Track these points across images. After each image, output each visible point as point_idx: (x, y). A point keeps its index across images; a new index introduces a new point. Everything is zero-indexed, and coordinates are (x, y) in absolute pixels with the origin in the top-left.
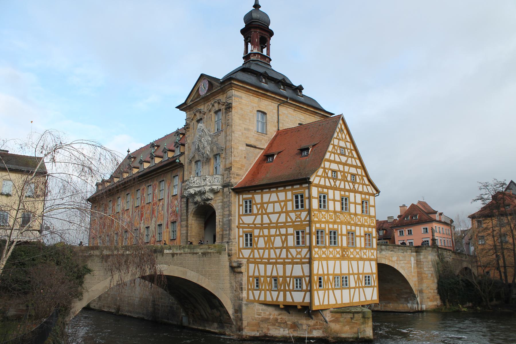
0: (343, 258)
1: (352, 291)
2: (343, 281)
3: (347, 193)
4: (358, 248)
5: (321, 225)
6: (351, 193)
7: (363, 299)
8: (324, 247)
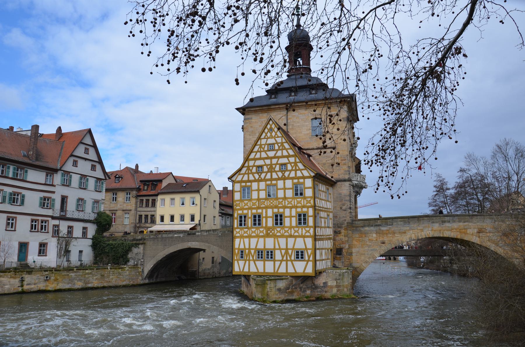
0: (267, 235)
1: (278, 264)
4: (287, 227)
6: (279, 182)
7: (291, 270)
8: (248, 228)
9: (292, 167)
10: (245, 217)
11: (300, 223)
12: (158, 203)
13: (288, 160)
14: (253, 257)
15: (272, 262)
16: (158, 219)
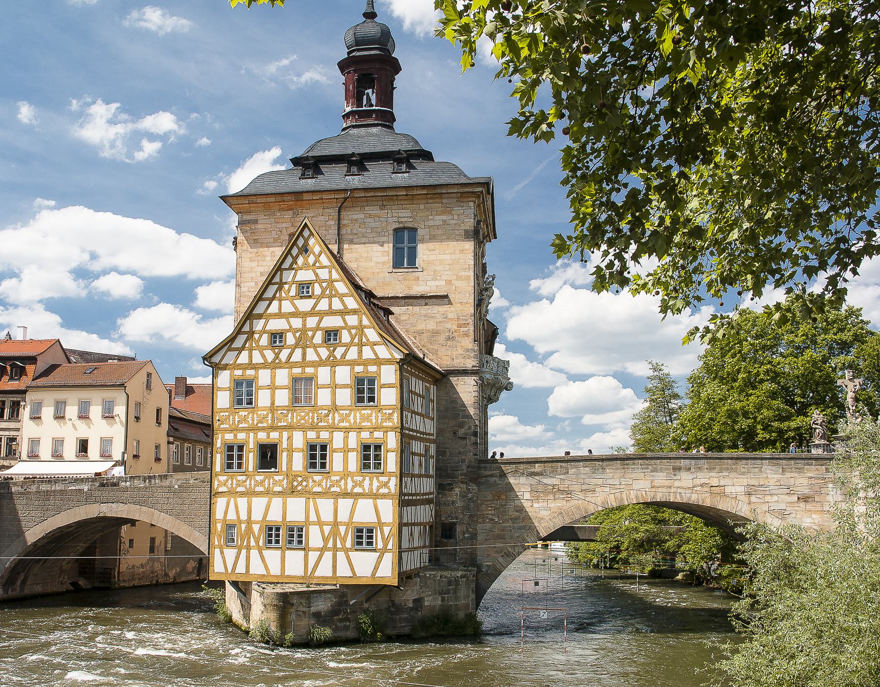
0: (292, 492)
1: (313, 556)
2: (293, 536)
3: (309, 370)
4: (337, 473)
5: (235, 436)
7: (344, 571)
9: (353, 338)
10: (241, 448)
11: (366, 466)
12: (25, 413)
13: (344, 320)
14: (257, 542)
15: (302, 553)
16: (24, 449)
